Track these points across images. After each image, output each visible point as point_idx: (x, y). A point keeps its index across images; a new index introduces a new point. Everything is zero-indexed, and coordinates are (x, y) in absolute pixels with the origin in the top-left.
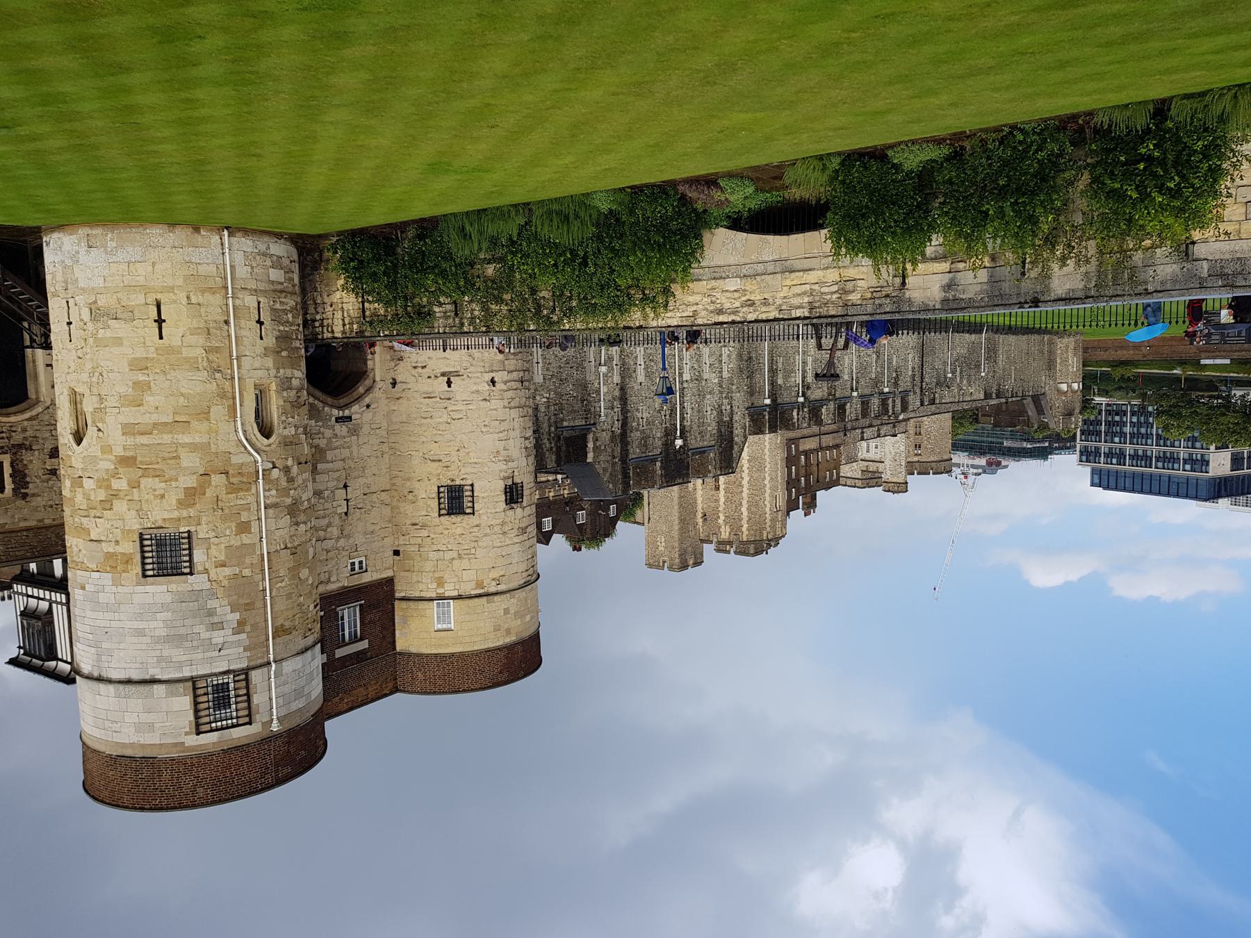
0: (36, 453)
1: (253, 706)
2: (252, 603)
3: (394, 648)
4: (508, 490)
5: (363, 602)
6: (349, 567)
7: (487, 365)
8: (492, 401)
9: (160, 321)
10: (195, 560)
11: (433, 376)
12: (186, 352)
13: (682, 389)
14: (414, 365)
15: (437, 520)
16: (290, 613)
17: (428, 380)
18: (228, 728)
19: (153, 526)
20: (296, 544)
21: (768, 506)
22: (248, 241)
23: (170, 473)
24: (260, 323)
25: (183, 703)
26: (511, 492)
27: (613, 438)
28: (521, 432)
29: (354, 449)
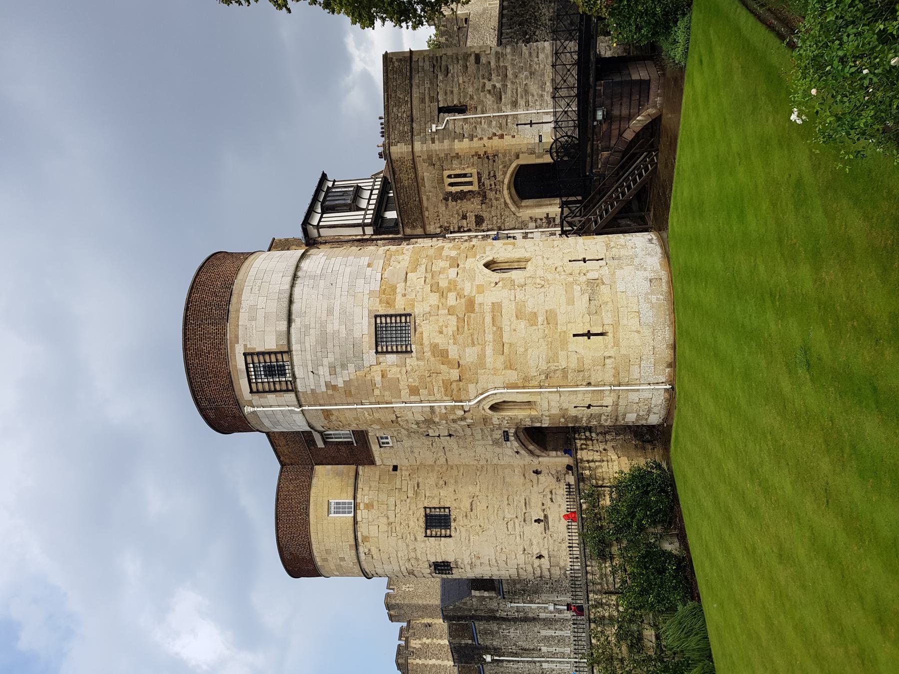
0: (480, 207)
3: (317, 464)
7: (555, 553)
9: (589, 335)
10: (388, 356)
11: (544, 507)
12: (562, 354)
13: (535, 662)
14: (553, 491)
16: (342, 419)
17: (540, 504)
18: (248, 376)
19: (417, 324)
20: (401, 423)
23: (460, 338)
24: (589, 407)
25: (271, 344)
26: (444, 566)
27: (493, 611)
28: (496, 575)
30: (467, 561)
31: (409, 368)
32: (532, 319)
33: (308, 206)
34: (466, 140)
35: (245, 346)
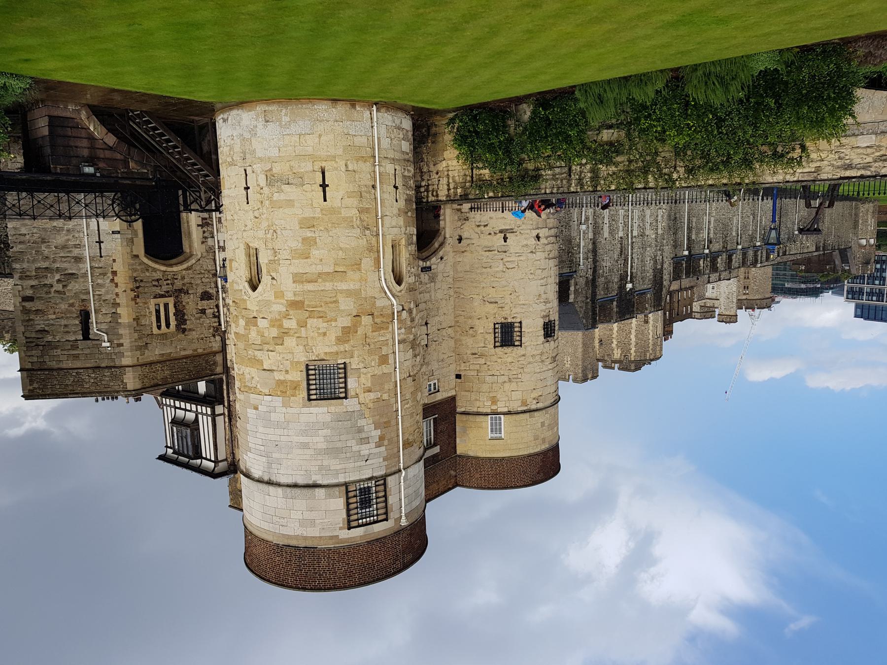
1: (389, 506)
2: (389, 422)
7: (535, 223)
8: (537, 253)
9: (324, 186)
10: (349, 386)
11: (493, 233)
12: (344, 213)
13: (632, 243)
14: (478, 224)
15: (493, 350)
16: (412, 429)
17: (489, 236)
18: (370, 523)
19: (316, 359)
21: (651, 334)
22: (389, 116)
23: (330, 315)
24: (396, 187)
25: (339, 503)
26: (547, 328)
27: (587, 283)
30: (542, 307)
31: (361, 365)
32: (309, 242)
33: (194, 473)
34: (119, 311)
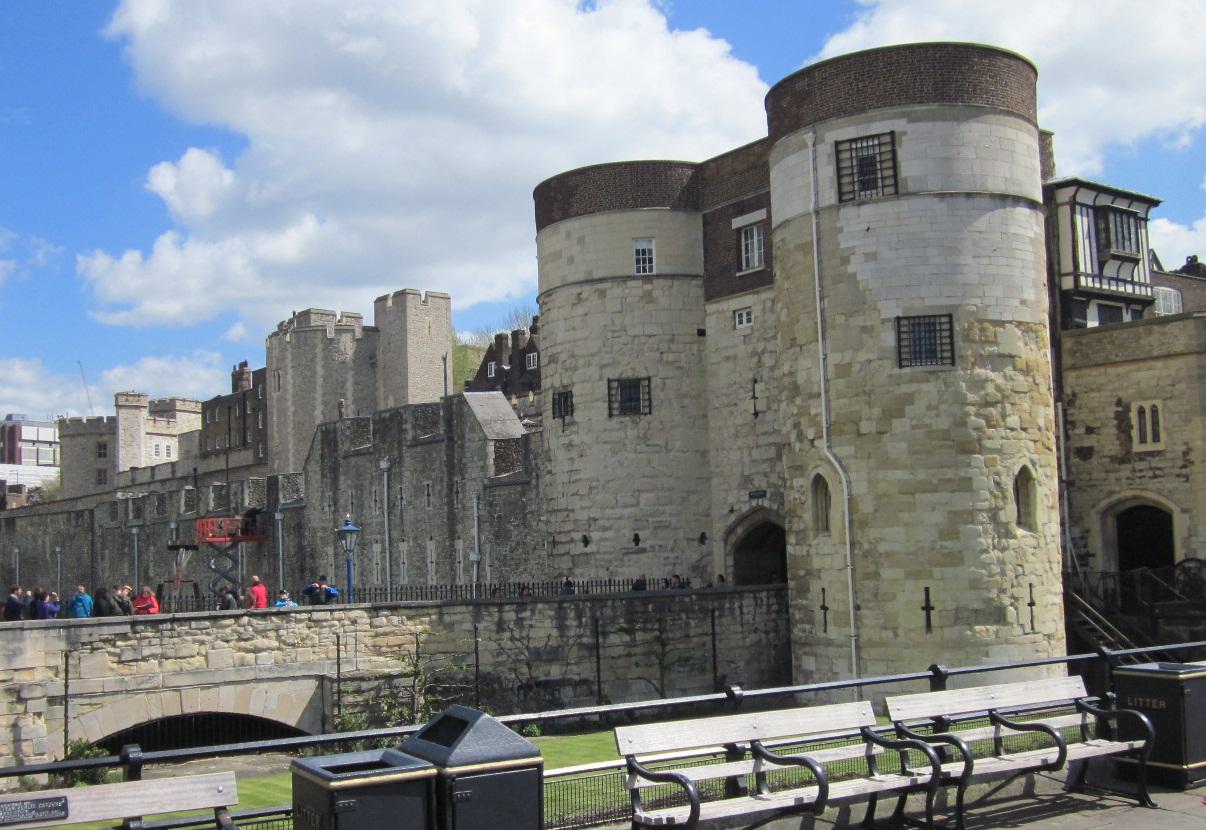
1: (834, 163)
3: (704, 216)
4: (570, 409)
5: (738, 274)
6: (753, 317)
7: (592, 562)
11: (657, 548)
12: (899, 573)
15: (651, 373)
20: (792, 350)
21: (289, 377)
24: (824, 608)
25: (909, 169)
26: (566, 407)
29: (746, 460)
30: (576, 439)
32: (950, 532)
33: (1106, 185)
35: (905, 133)
